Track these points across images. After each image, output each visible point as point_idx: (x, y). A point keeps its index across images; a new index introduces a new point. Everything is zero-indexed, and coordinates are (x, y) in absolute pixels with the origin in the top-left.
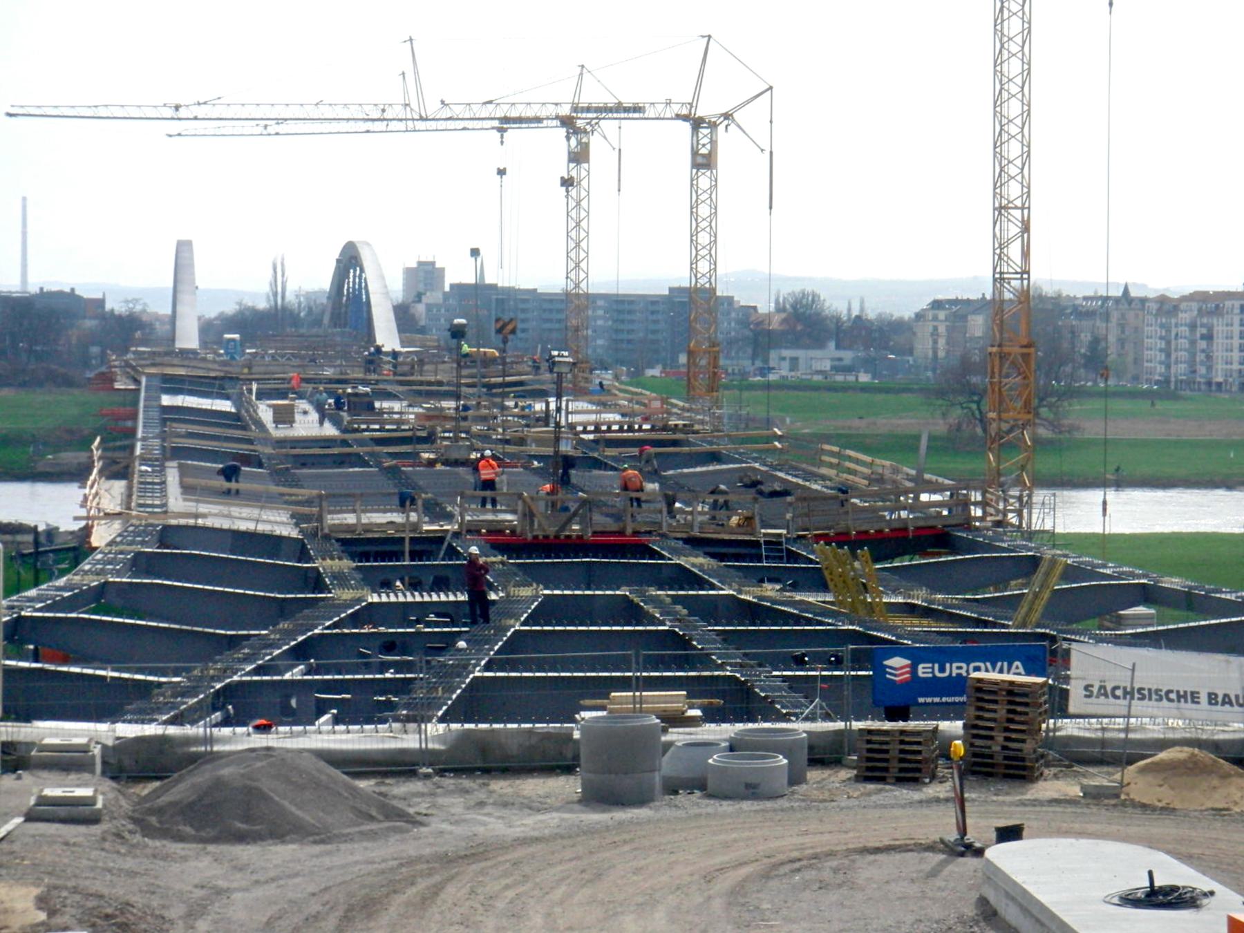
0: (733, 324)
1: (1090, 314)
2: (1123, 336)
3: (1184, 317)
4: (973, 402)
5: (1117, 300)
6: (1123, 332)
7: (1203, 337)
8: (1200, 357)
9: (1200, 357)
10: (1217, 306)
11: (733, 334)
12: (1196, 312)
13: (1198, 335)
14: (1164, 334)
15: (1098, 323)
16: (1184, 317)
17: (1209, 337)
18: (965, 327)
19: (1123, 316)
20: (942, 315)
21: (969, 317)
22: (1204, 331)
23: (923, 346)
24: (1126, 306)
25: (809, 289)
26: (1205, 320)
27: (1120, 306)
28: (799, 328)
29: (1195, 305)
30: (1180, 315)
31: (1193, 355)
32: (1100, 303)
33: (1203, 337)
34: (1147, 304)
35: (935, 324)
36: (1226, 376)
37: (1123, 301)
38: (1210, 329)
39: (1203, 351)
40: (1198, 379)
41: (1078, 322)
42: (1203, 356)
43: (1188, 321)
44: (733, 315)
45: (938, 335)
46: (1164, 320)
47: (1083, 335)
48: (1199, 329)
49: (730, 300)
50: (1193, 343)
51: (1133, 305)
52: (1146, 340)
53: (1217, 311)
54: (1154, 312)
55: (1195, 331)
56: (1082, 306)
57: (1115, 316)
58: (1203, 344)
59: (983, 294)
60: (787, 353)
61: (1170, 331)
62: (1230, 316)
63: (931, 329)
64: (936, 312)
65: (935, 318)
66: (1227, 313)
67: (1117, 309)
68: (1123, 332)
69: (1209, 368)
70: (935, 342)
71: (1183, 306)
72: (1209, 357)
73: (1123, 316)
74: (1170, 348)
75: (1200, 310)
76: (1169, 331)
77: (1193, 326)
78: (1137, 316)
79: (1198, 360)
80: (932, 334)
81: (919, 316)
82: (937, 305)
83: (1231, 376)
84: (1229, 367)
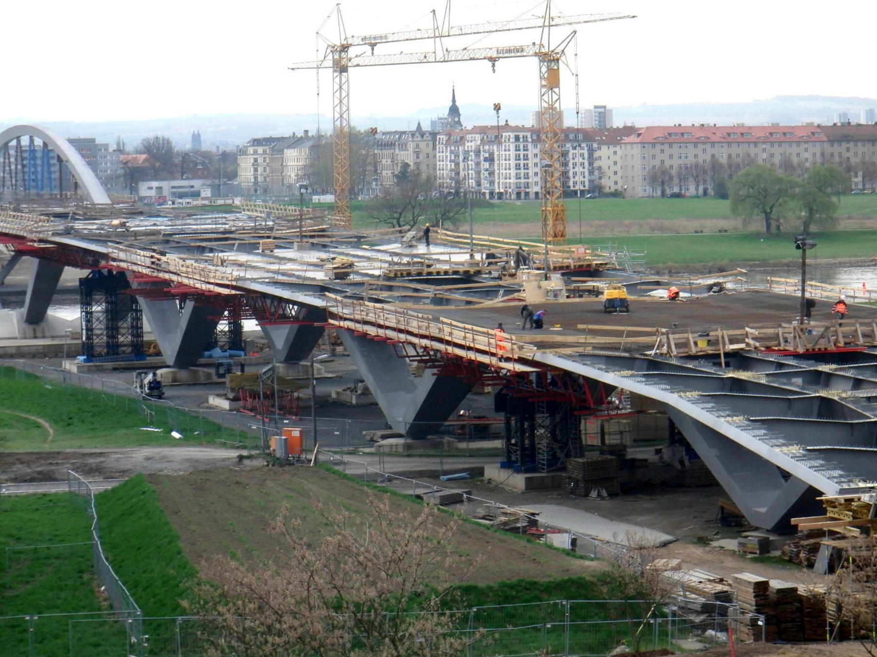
0: (109, 164)
1: (390, 145)
2: (418, 160)
3: (470, 145)
4: (394, 218)
5: (413, 135)
6: (418, 157)
7: (486, 160)
8: (484, 174)
9: (484, 174)
10: (497, 137)
11: (109, 172)
12: (479, 142)
13: (482, 158)
14: (453, 158)
15: (397, 151)
16: (470, 145)
17: (491, 159)
18: (282, 158)
19: (417, 146)
20: (260, 150)
21: (285, 151)
22: (487, 155)
23: (246, 173)
24: (420, 138)
25: (160, 134)
26: (487, 147)
27: (415, 139)
28: (158, 164)
29: (478, 137)
30: (467, 144)
31: (478, 173)
32: (397, 136)
33: (486, 160)
34: (438, 137)
35: (255, 156)
36: (506, 187)
37: (417, 134)
38: (492, 154)
39: (487, 170)
40: (483, 191)
41: (379, 151)
42: (486, 173)
43: (473, 148)
44: (108, 157)
45: (257, 165)
46: (453, 148)
47: (384, 161)
48: (482, 153)
49: (106, 147)
50: (478, 164)
51: (425, 138)
52: (438, 163)
53: (497, 140)
54: (444, 142)
55: (479, 155)
56: (382, 139)
57: (411, 146)
58: (487, 165)
59: (294, 133)
60: (155, 184)
61: (458, 156)
62: (507, 144)
63: (252, 161)
64: (256, 148)
65: (255, 152)
66: (505, 141)
67: (413, 141)
68: (418, 157)
69: (492, 183)
70: (256, 170)
71: (469, 137)
72: (492, 174)
73: (417, 146)
74: (459, 168)
75: (482, 140)
76: (457, 156)
77: (478, 153)
78: (428, 145)
79: (482, 176)
80: (253, 165)
81: (243, 152)
82: (257, 142)
83: (510, 188)
84: (508, 181)
